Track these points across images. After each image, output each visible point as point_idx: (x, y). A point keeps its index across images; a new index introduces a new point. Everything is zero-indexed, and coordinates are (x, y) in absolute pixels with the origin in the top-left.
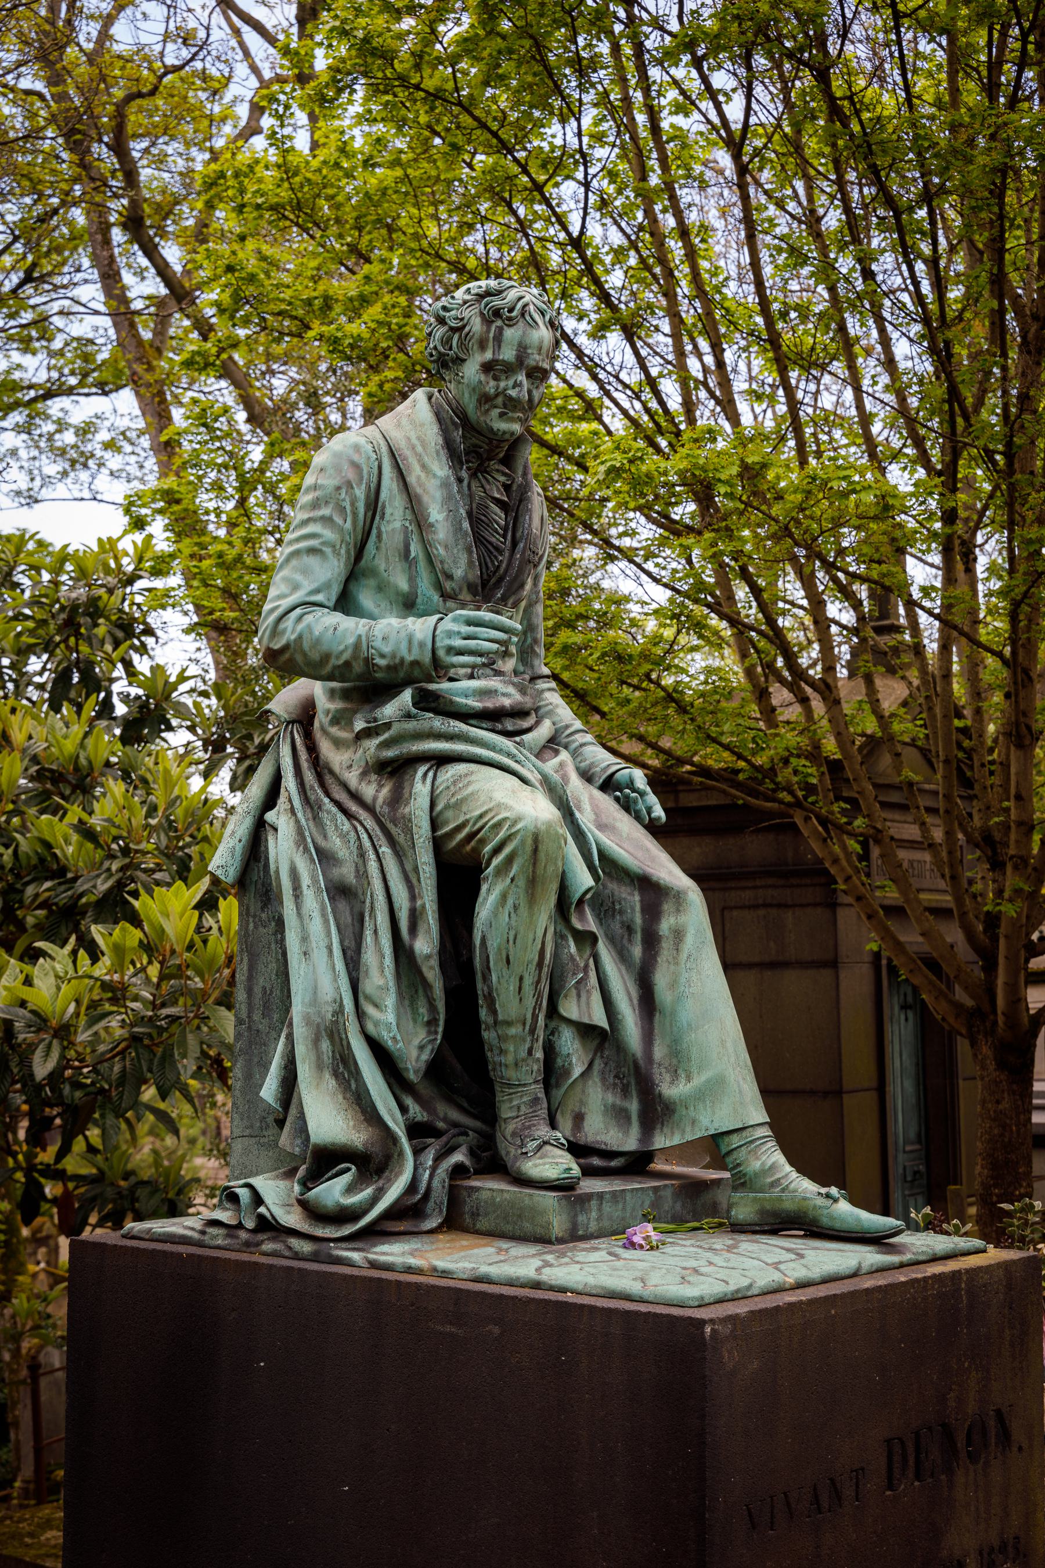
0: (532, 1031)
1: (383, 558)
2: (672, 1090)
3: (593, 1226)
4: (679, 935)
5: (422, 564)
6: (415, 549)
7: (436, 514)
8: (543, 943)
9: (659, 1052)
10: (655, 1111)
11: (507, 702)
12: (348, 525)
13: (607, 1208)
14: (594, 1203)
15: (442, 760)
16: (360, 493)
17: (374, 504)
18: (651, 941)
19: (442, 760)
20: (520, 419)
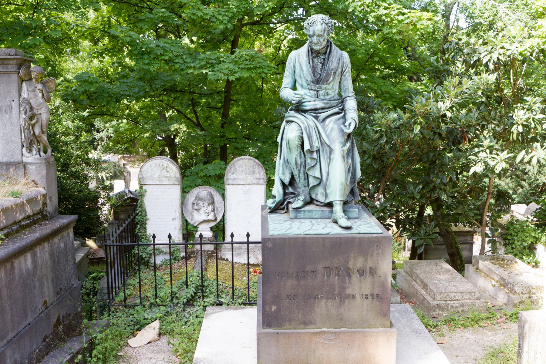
0: (299, 177)
1: (297, 78)
2: (328, 191)
3: (302, 217)
4: (333, 159)
5: (303, 78)
6: (302, 75)
7: (304, 68)
8: (296, 161)
9: (328, 183)
10: (326, 196)
11: (318, 107)
12: (291, 71)
13: (306, 213)
14: (302, 213)
15: (292, 122)
16: (292, 64)
17: (294, 67)
18: (330, 159)
19: (292, 122)
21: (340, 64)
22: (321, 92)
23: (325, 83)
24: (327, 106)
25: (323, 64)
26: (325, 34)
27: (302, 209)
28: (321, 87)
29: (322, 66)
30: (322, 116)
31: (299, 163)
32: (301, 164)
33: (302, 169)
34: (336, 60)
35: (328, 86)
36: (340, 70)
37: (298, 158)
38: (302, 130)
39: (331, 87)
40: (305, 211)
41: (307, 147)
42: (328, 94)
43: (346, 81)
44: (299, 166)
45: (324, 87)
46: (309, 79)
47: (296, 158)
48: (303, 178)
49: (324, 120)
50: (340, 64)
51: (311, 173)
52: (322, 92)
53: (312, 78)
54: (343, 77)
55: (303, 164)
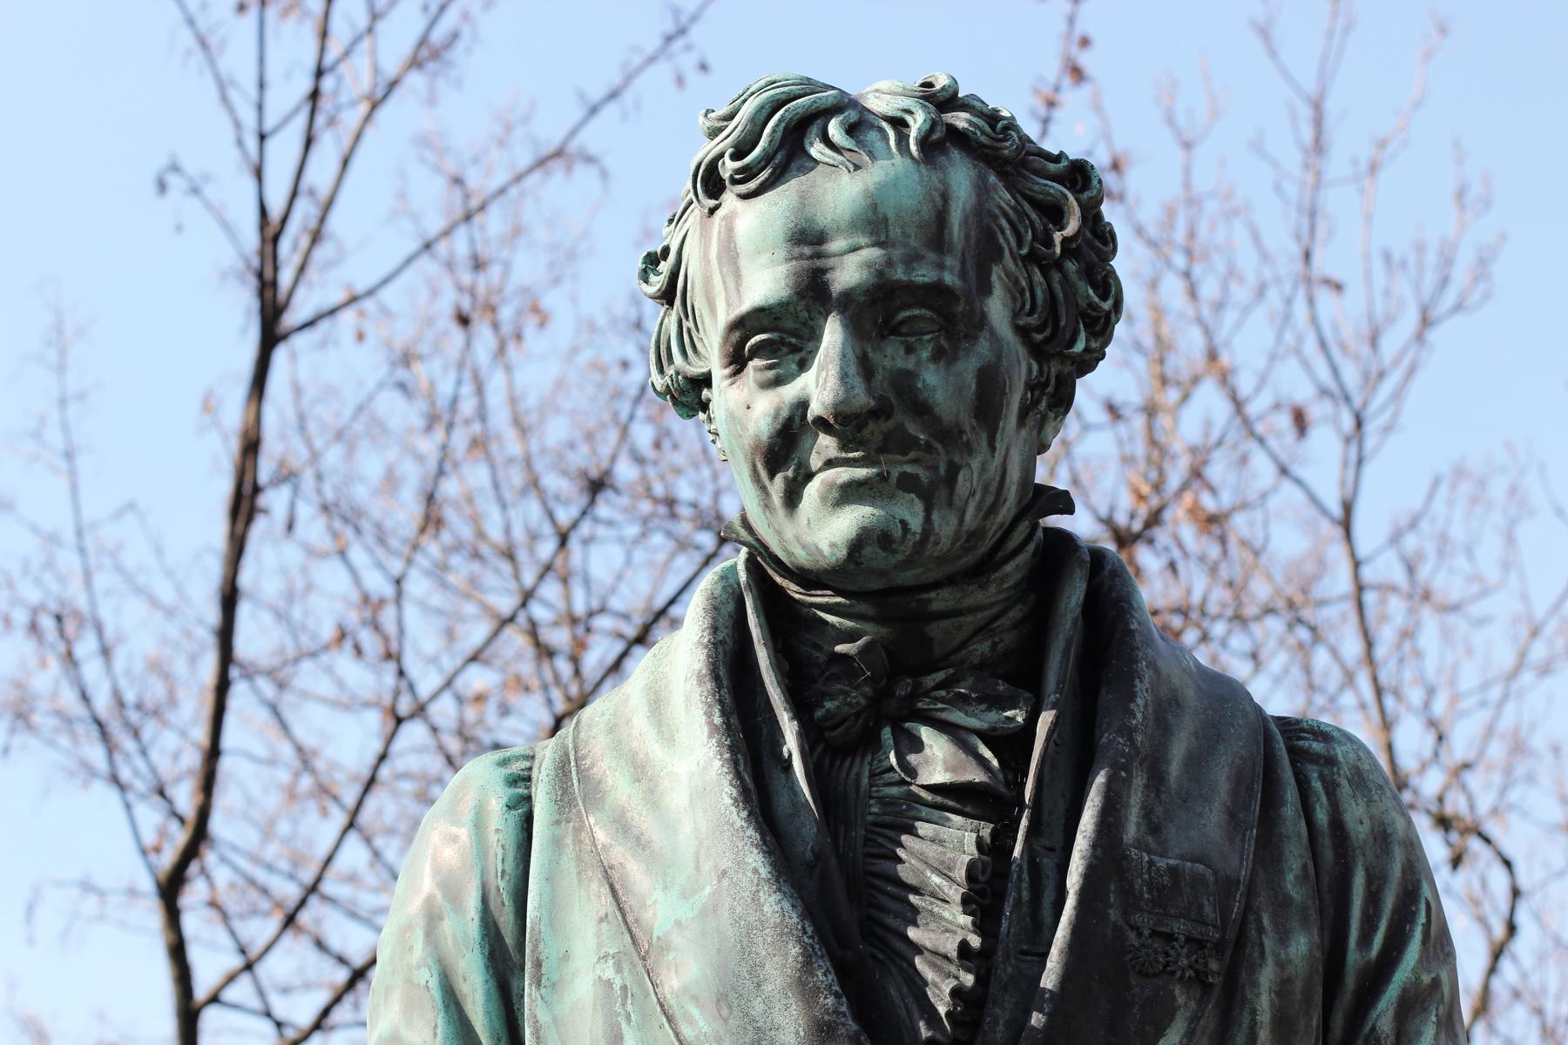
20: (908, 483)
21: (1295, 858)
26: (997, 308)
34: (1221, 776)
50: (1295, 858)
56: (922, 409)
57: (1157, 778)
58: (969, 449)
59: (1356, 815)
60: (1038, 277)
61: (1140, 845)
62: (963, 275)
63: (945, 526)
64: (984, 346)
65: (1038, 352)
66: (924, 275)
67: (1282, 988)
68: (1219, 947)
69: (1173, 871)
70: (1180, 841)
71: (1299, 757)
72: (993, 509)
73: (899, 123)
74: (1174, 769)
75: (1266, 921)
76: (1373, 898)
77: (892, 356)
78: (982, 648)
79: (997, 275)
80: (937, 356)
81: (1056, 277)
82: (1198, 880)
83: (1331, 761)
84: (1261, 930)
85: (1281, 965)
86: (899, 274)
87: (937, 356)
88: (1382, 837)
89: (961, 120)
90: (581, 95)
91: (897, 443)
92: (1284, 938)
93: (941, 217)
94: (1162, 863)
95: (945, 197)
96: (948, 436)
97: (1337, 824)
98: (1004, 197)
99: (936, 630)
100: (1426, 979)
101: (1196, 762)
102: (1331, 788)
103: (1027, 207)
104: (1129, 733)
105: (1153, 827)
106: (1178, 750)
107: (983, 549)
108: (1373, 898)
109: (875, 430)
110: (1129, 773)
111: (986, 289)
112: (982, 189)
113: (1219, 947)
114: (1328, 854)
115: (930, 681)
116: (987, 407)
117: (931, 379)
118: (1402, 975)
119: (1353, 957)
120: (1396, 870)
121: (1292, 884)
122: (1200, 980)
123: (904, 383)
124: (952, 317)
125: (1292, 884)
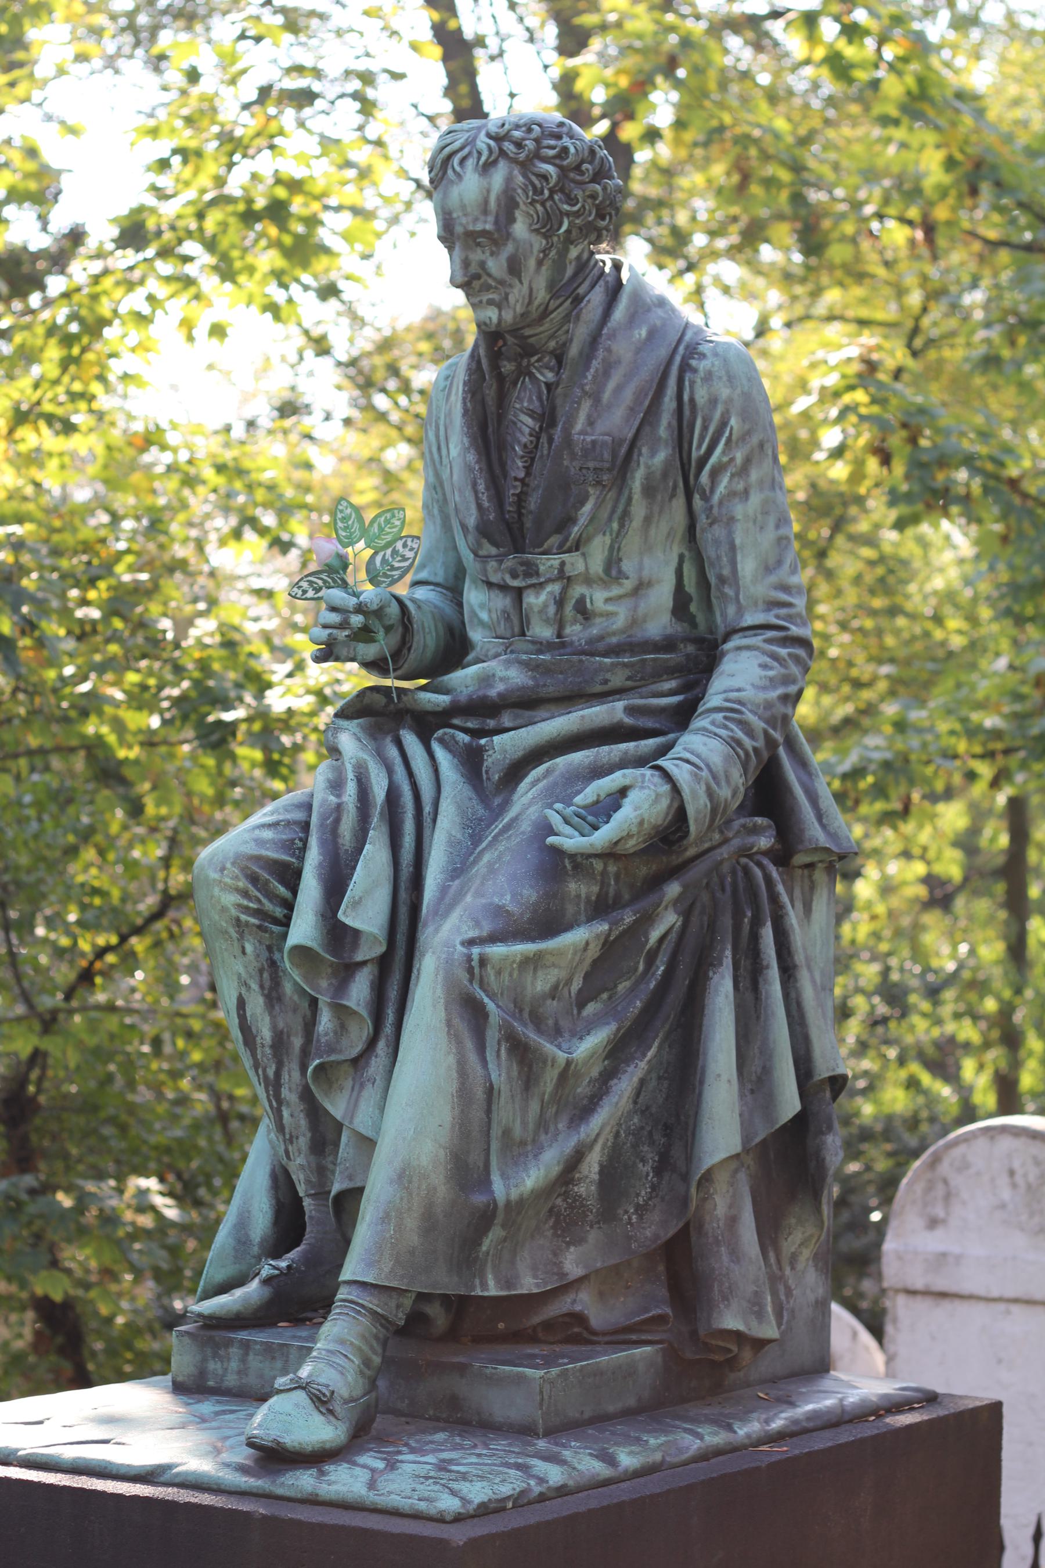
13: (254, 1362)
14: (234, 1351)
20: (491, 302)
22: (534, 600)
23: (554, 540)
24: (551, 687)
25: (547, 418)
26: (520, 228)
27: (243, 1335)
28: (530, 570)
29: (537, 435)
30: (506, 745)
31: (265, 1033)
32: (280, 1043)
33: (292, 1076)
34: (628, 395)
35: (575, 563)
36: (656, 458)
37: (256, 1005)
38: (306, 826)
39: (597, 566)
40: (246, 1346)
41: (304, 928)
42: (583, 611)
43: (718, 531)
44: (265, 1053)
45: (548, 564)
46: (472, 521)
47: (241, 1004)
48: (303, 1142)
49: (516, 771)
51: (336, 1107)
52: (543, 597)
53: (479, 507)
54: (697, 502)
55: (297, 1042)
56: (489, 275)
57: (597, 399)
58: (511, 286)
59: (701, 395)
60: (539, 207)
61: (583, 432)
62: (496, 222)
63: (508, 316)
64: (509, 249)
65: (546, 236)
66: (479, 227)
67: (648, 477)
68: (610, 470)
69: (594, 442)
70: (601, 427)
71: (685, 367)
72: (530, 303)
73: (480, 154)
74: (606, 395)
75: (644, 450)
76: (705, 428)
77: (477, 256)
78: (552, 344)
79: (518, 214)
80: (492, 254)
81: (548, 204)
82: (604, 444)
83: (695, 371)
84: (640, 454)
85: (648, 467)
86: (471, 228)
87: (492, 254)
88: (713, 401)
89: (508, 146)
90: (509, 36)
91: (487, 288)
92: (653, 453)
93: (486, 201)
94: (589, 439)
95: (488, 191)
96: (502, 282)
97: (692, 400)
98: (520, 179)
99: (532, 340)
100: (725, 459)
101: (619, 389)
102: (692, 383)
103: (533, 178)
104: (582, 387)
105: (591, 423)
106: (611, 385)
107: (535, 315)
108: (705, 428)
109: (476, 284)
110: (579, 403)
111: (512, 220)
112: (509, 180)
113: (610, 470)
114: (687, 412)
115: (534, 359)
116: (515, 267)
117: (492, 265)
118: (713, 460)
119: (695, 455)
120: (717, 415)
121: (663, 431)
122: (599, 483)
123: (482, 264)
124: (497, 237)
125: (663, 431)
